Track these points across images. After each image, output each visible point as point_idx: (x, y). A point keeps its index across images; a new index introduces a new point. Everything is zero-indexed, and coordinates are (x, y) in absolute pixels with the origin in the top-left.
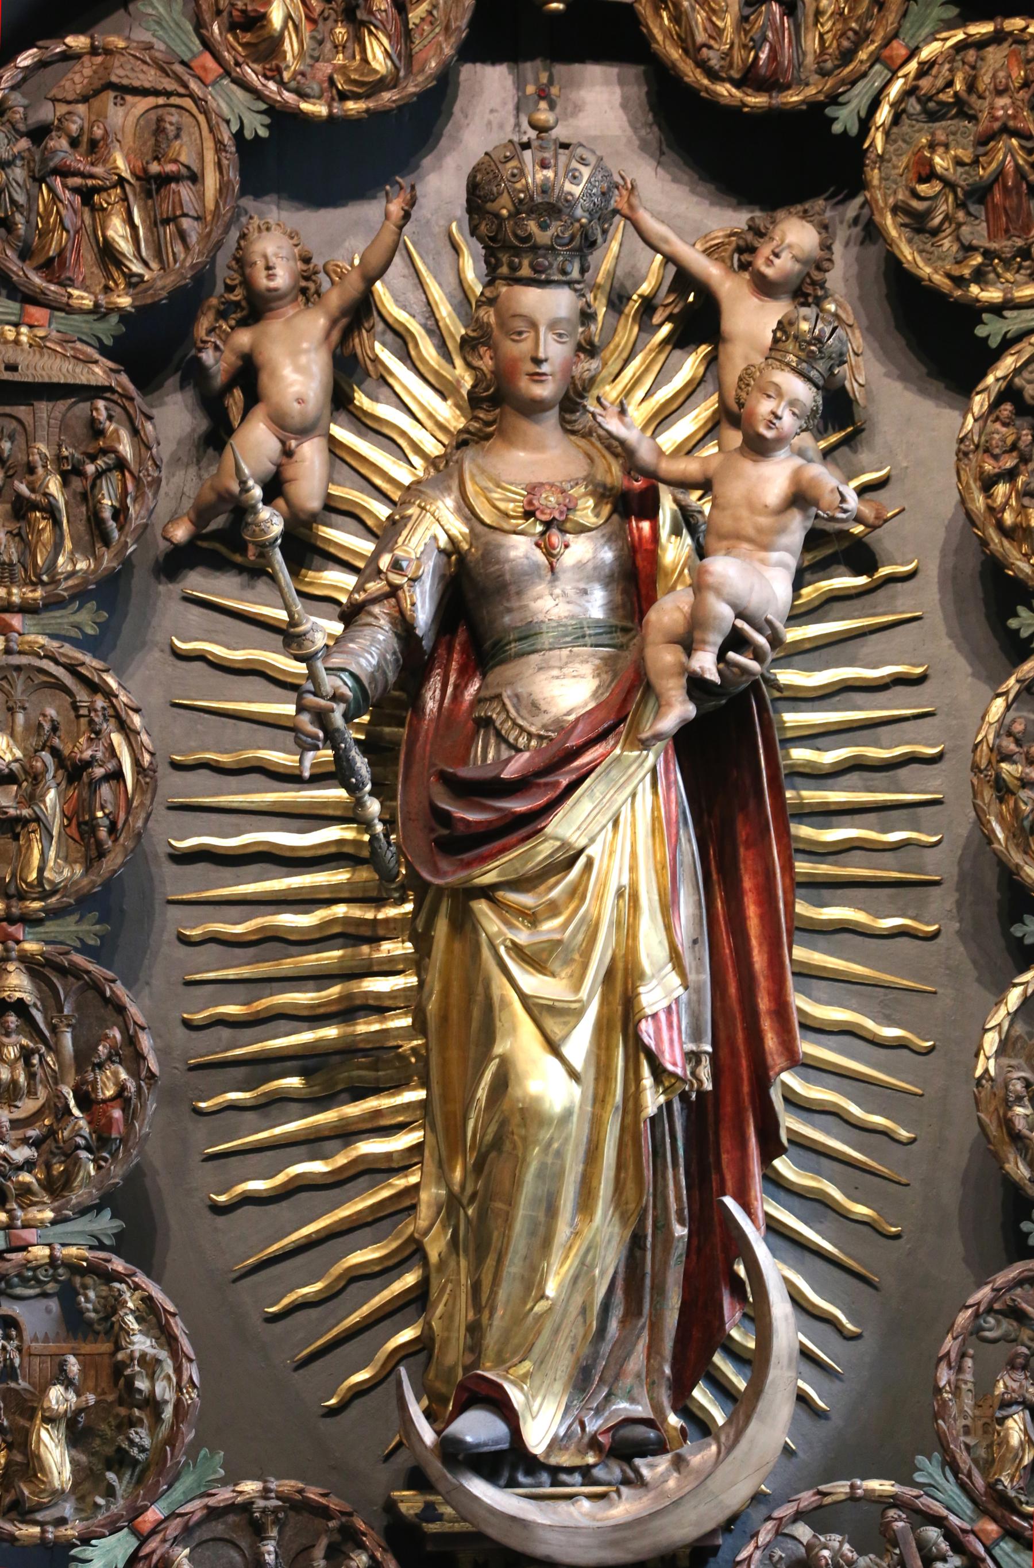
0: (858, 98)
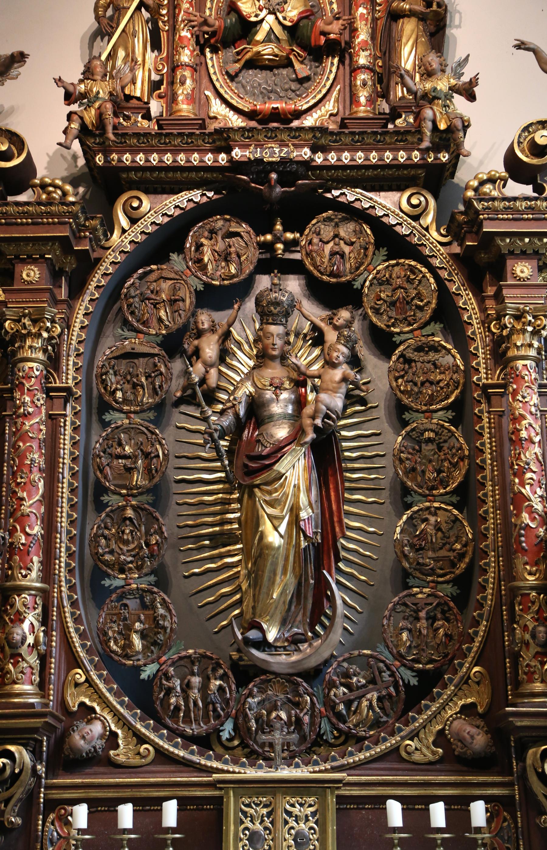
0: (361, 279)
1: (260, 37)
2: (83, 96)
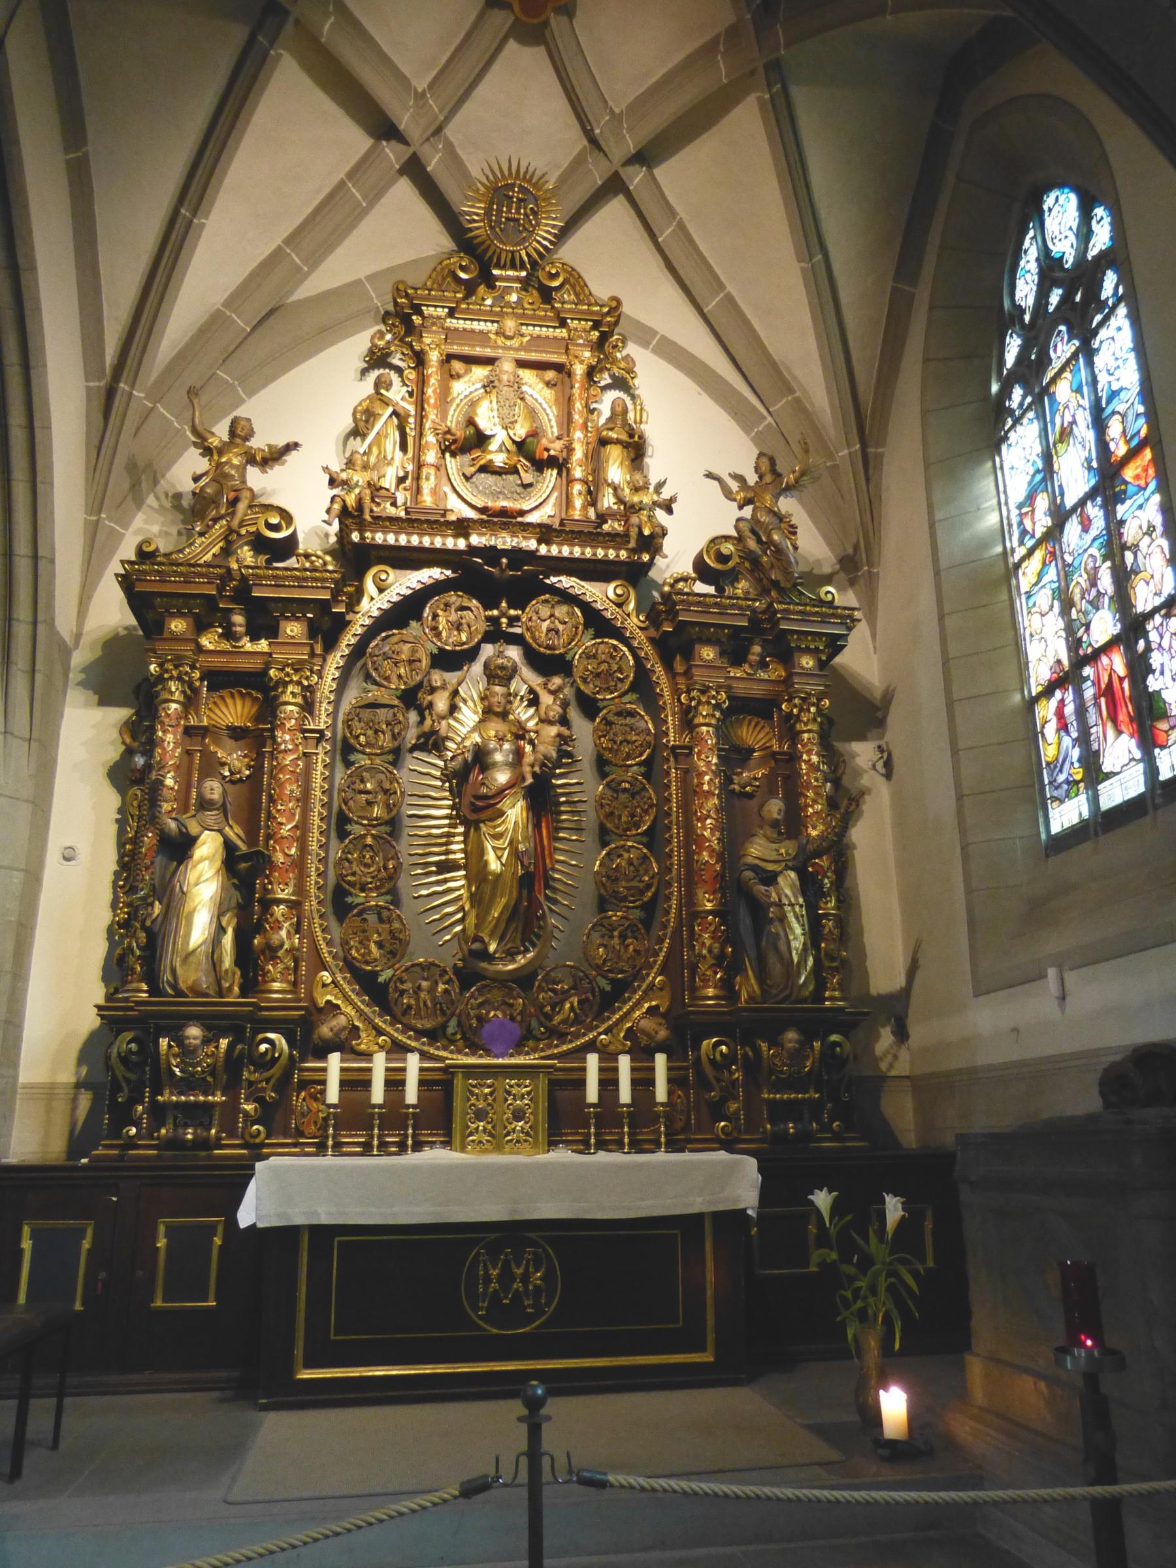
0: (572, 653)
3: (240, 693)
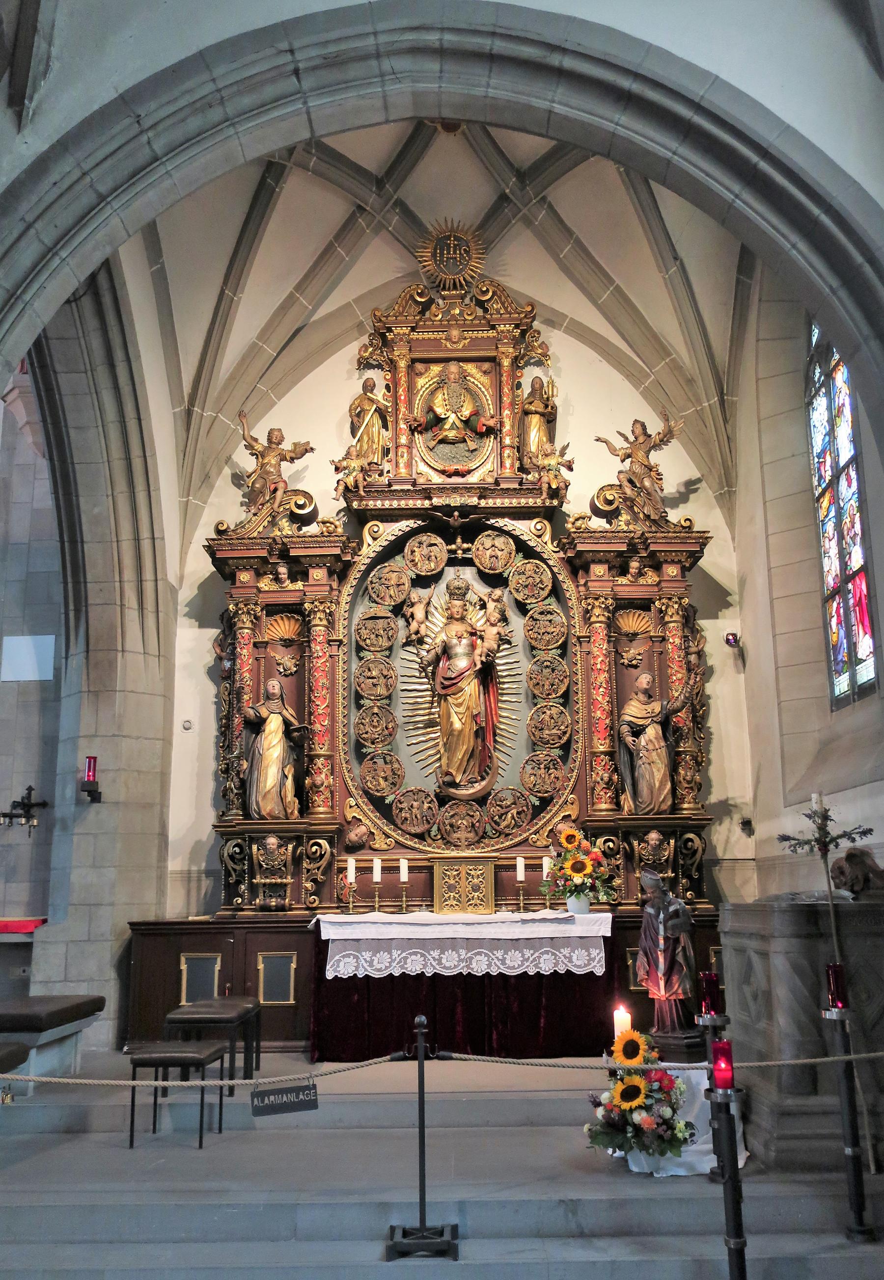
0: (507, 572)
1: (447, 426)
2: (345, 468)
3: (287, 616)
